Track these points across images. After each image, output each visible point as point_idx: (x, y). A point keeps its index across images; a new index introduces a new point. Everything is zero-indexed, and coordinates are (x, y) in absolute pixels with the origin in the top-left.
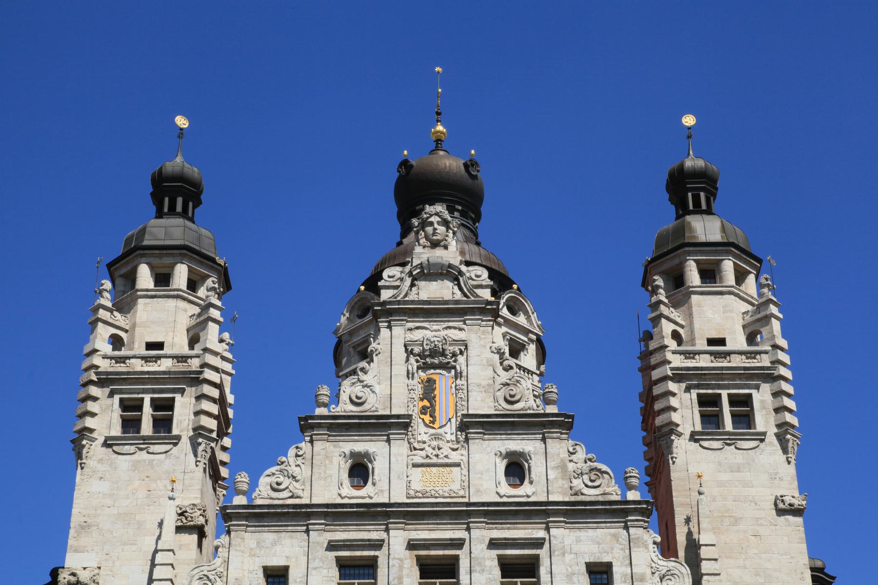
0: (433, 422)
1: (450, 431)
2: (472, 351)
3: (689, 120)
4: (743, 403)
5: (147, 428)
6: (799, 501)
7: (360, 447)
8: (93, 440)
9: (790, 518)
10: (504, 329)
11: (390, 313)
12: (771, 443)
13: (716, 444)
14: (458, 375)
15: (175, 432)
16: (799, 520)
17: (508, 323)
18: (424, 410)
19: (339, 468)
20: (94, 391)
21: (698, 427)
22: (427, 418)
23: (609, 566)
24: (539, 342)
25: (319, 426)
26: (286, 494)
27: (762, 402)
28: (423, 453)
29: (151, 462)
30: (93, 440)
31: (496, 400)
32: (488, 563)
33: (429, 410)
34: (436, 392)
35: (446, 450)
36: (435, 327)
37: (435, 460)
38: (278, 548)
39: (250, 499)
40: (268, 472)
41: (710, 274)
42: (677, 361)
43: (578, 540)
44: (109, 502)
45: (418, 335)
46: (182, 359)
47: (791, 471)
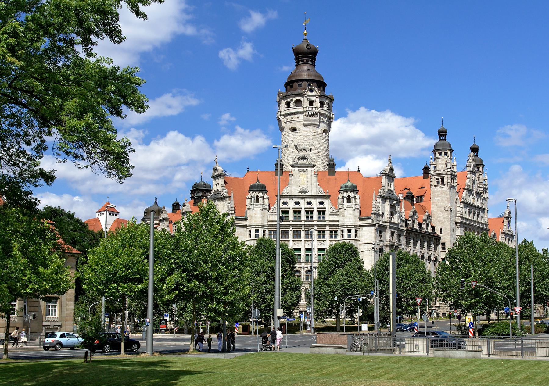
10: (308, 97)
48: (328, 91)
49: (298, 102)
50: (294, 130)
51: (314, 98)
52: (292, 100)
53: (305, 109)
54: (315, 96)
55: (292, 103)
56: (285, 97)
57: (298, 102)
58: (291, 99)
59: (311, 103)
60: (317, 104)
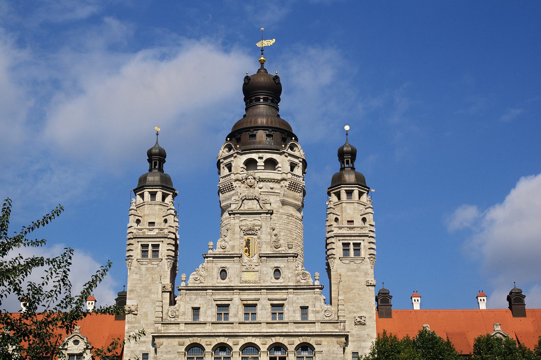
0: (249, 256)
1: (255, 258)
2: (264, 229)
3: (347, 128)
4: (357, 245)
5: (150, 253)
6: (374, 283)
7: (223, 265)
8: (132, 260)
9: (370, 287)
10: (289, 158)
11: (234, 214)
12: (366, 262)
13: (347, 262)
14: (259, 238)
15: (160, 257)
16: (373, 288)
17: (290, 155)
18: (246, 251)
19: (216, 273)
20: (132, 241)
21: (342, 256)
22: (247, 254)
23: (307, 308)
24: (305, 163)
25: (210, 257)
26: (199, 282)
27: (364, 246)
28: (245, 267)
29: (153, 268)
30: (132, 260)
31: (271, 247)
32: (267, 307)
33: (248, 251)
34: (251, 244)
35: (253, 266)
36: (250, 220)
37: (250, 270)
38: (197, 301)
39: (187, 284)
40: (193, 274)
41: (349, 193)
42: (336, 231)
43: (298, 299)
44: (139, 282)
45: (243, 223)
46: (162, 230)
47: (371, 271)
49: (271, 164)
51: (296, 161)
52: (261, 158)
53: (284, 176)
54: (297, 158)
55: (261, 163)
57: (271, 164)
58: (261, 155)
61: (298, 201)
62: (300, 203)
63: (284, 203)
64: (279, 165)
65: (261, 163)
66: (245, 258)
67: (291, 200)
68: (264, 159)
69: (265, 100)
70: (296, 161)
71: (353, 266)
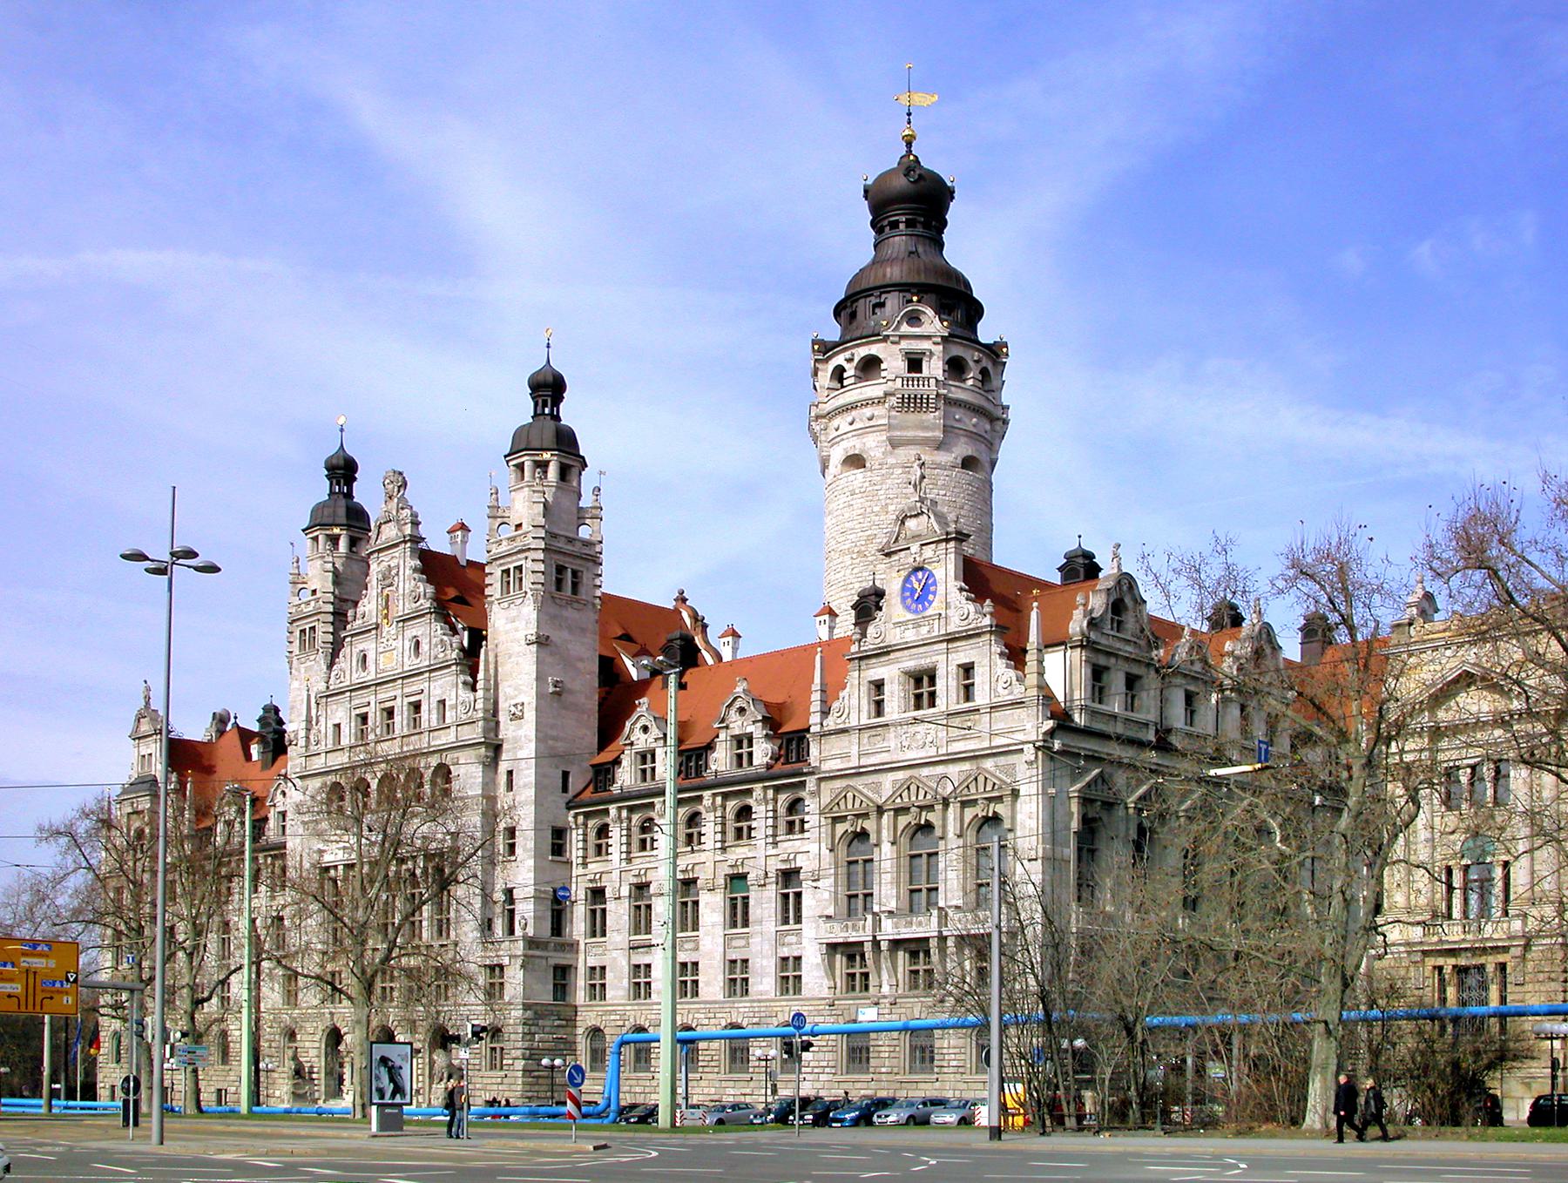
10: (904, 344)
33: (386, 616)
48: (986, 332)
49: (870, 366)
50: (855, 461)
51: (925, 345)
52: (850, 360)
53: (890, 386)
54: (928, 337)
55: (850, 370)
56: (825, 349)
57: (870, 366)
58: (847, 354)
59: (915, 364)
60: (934, 368)
61: (932, 430)
62: (939, 434)
63: (894, 444)
64: (883, 366)
65: (850, 370)
66: (386, 628)
67: (910, 434)
68: (856, 360)
69: (909, 224)
70: (925, 345)
71: (513, 611)
